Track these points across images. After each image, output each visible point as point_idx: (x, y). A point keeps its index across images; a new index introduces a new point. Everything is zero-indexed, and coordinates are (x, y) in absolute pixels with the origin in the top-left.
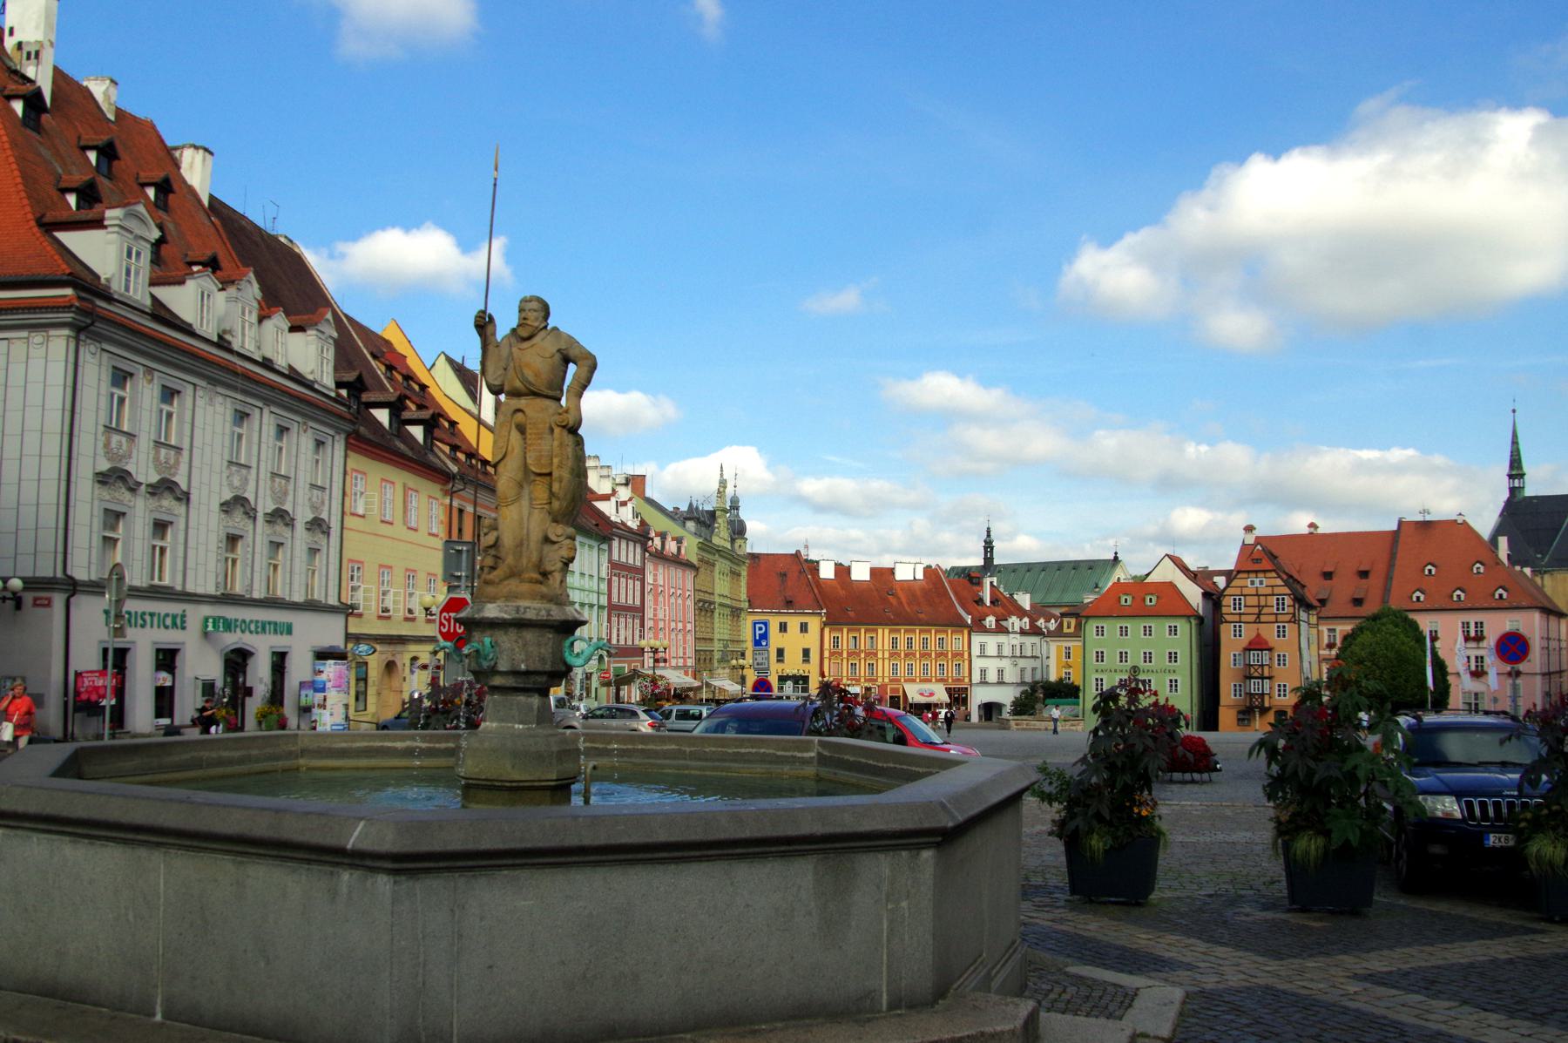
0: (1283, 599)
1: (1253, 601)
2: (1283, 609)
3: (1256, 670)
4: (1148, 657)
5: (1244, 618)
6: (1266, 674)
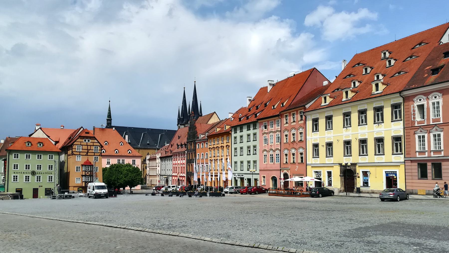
0: (97, 147)
1: (85, 147)
2: (97, 151)
3: (88, 173)
4: (39, 167)
5: (81, 154)
6: (91, 175)
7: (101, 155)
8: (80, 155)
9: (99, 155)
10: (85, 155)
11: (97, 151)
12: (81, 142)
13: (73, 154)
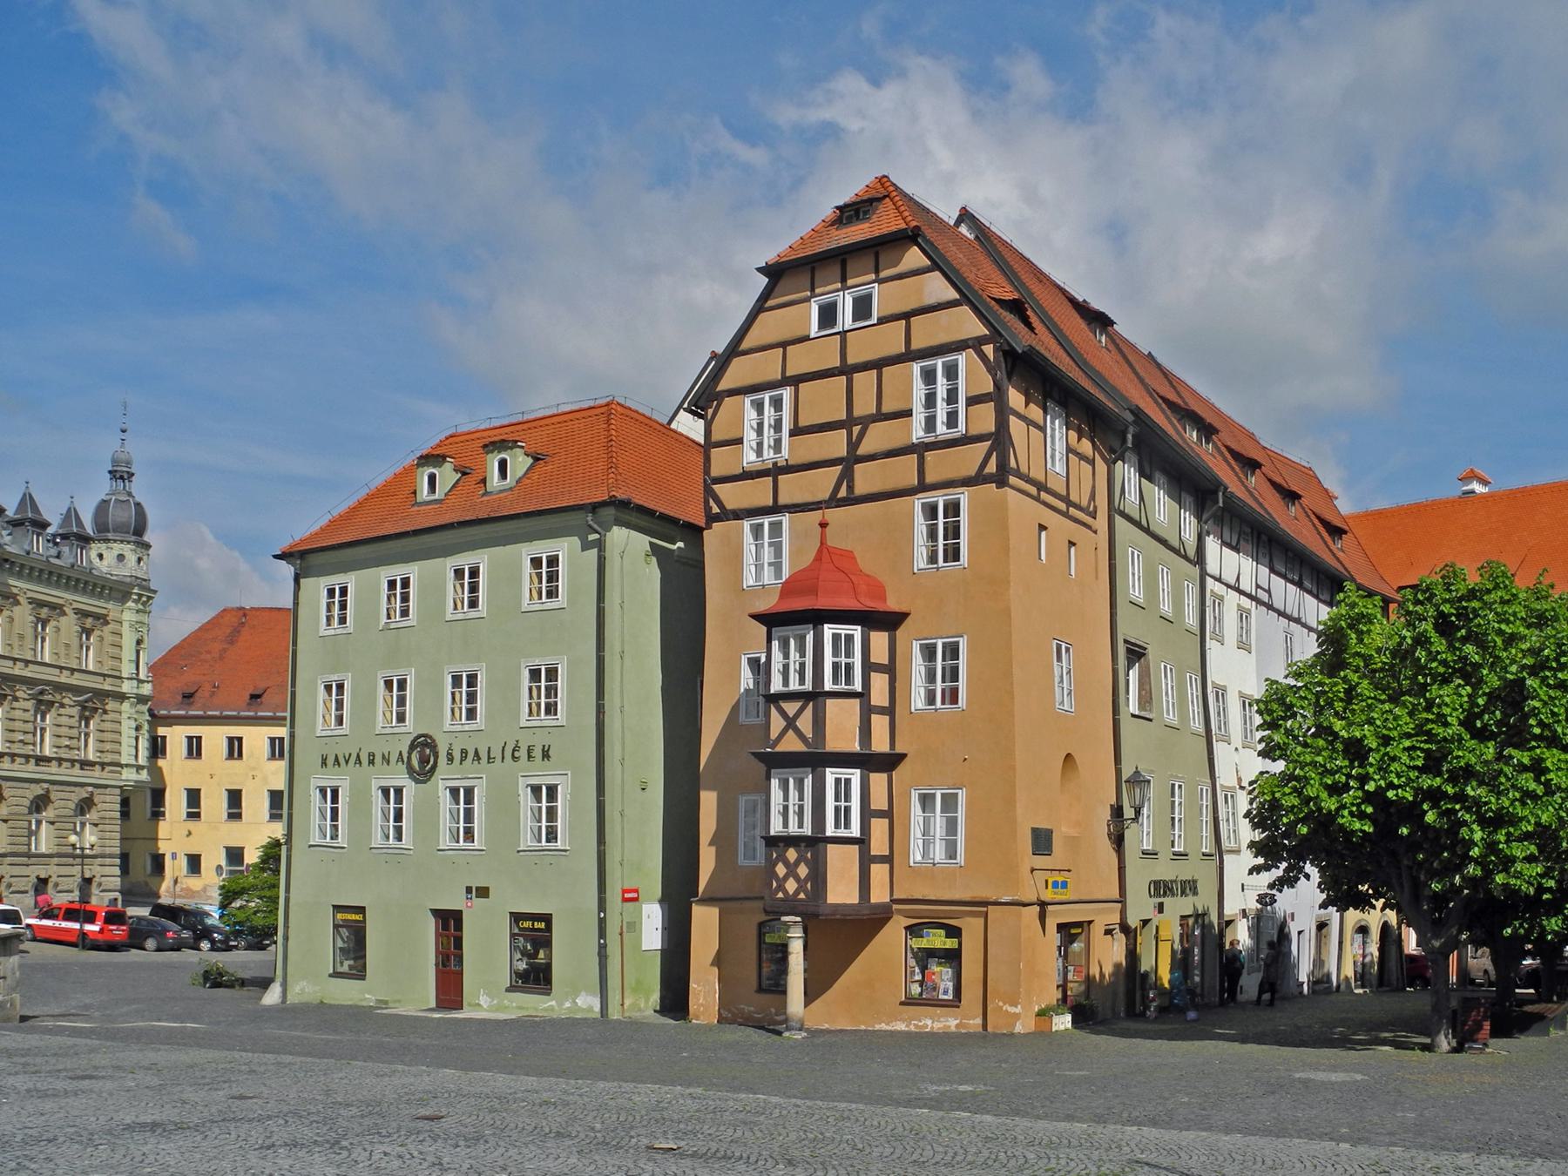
3: (791, 723)
5: (793, 488)
7: (992, 467)
8: (775, 509)
9: (972, 471)
10: (826, 496)
11: (952, 420)
12: (784, 345)
13: (716, 510)
